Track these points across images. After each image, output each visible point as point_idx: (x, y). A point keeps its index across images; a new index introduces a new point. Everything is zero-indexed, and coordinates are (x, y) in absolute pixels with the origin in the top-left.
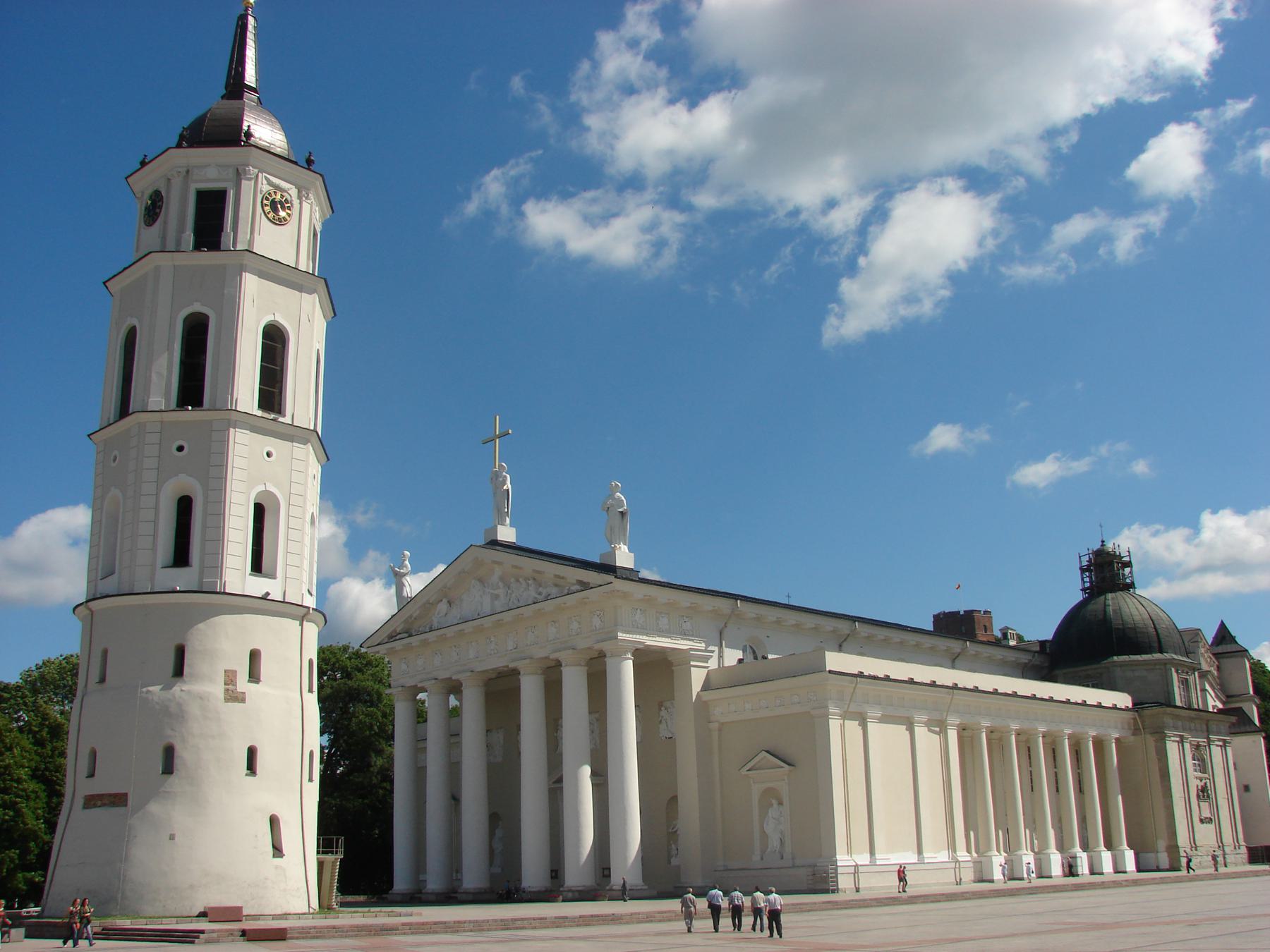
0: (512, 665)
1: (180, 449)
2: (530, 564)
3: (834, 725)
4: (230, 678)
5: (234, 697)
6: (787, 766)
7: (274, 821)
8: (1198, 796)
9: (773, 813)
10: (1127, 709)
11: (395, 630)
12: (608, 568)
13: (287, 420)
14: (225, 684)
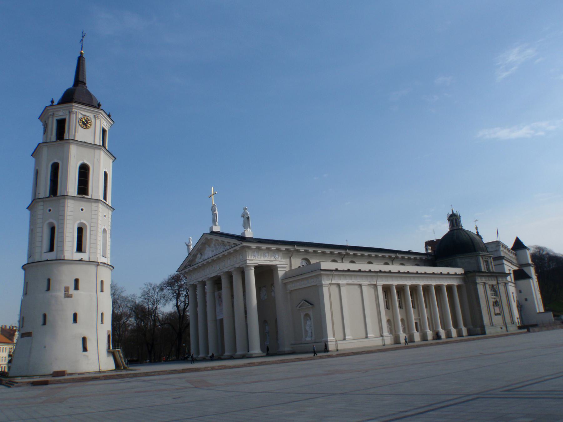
0: (219, 275)
1: (50, 210)
2: (220, 239)
3: (325, 290)
4: (67, 289)
5: (68, 296)
6: (310, 305)
7: (84, 339)
8: (493, 305)
9: (308, 323)
10: (462, 274)
11: (186, 265)
12: (242, 239)
13: (89, 197)
14: (65, 291)
